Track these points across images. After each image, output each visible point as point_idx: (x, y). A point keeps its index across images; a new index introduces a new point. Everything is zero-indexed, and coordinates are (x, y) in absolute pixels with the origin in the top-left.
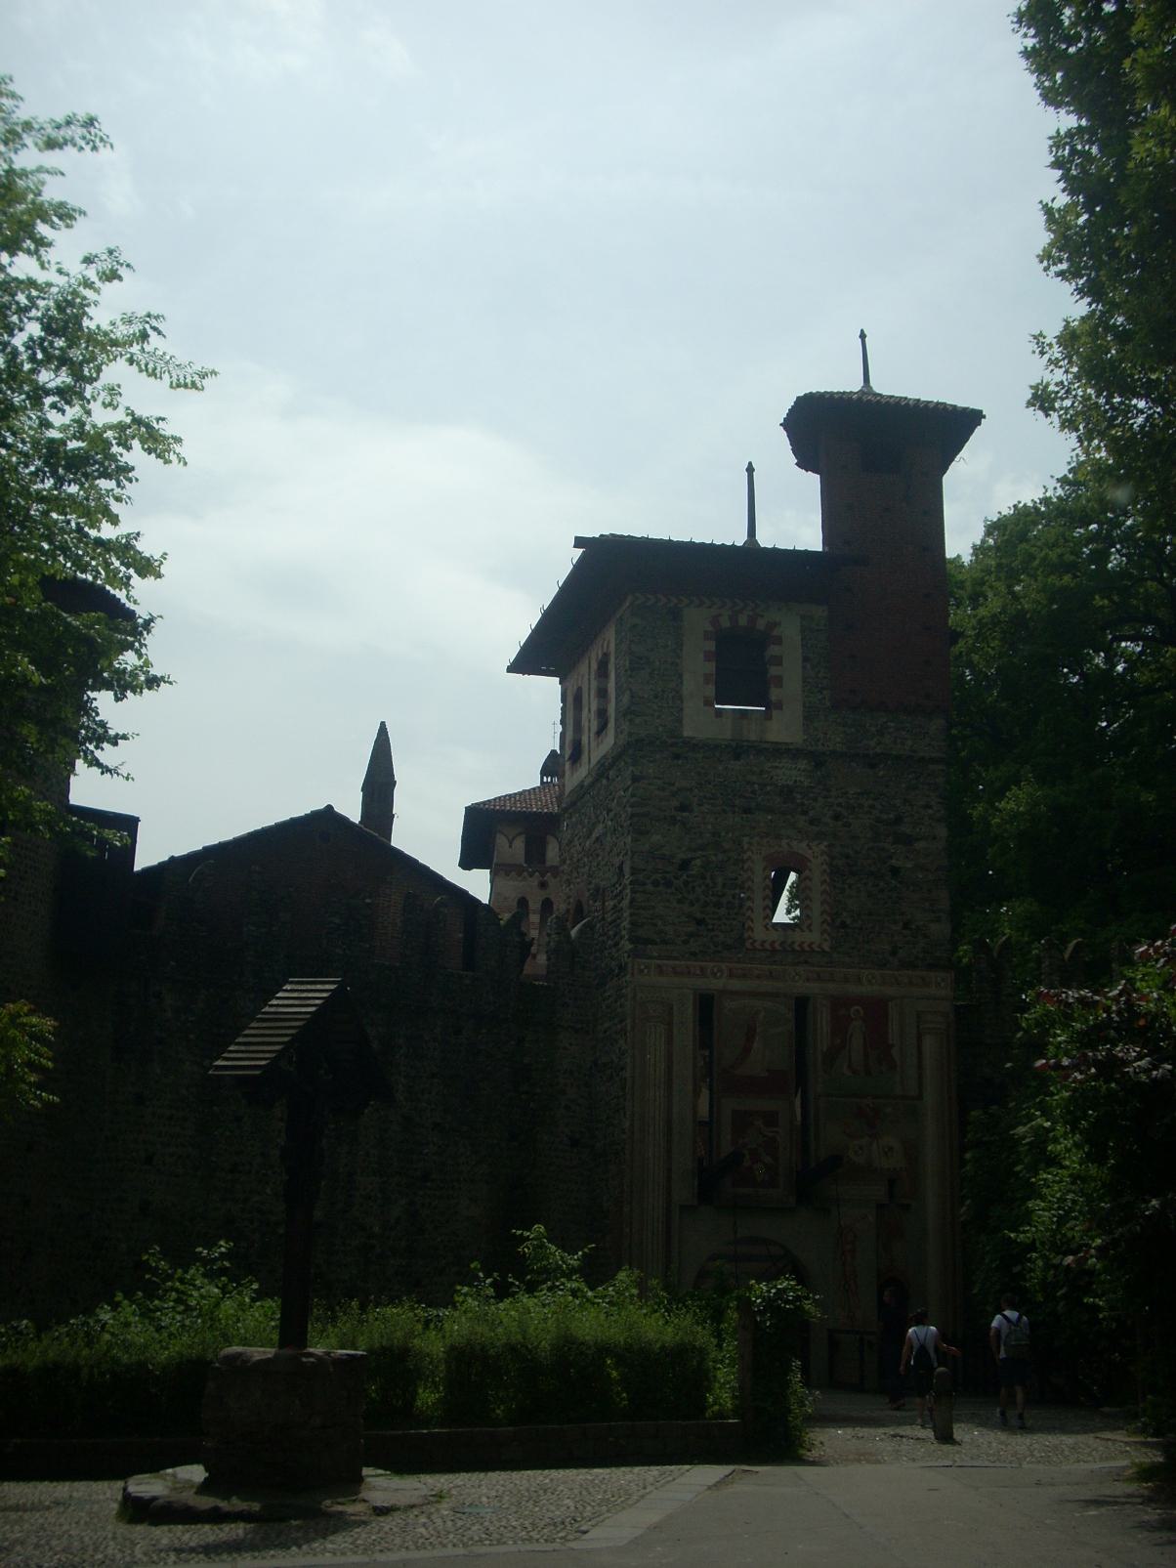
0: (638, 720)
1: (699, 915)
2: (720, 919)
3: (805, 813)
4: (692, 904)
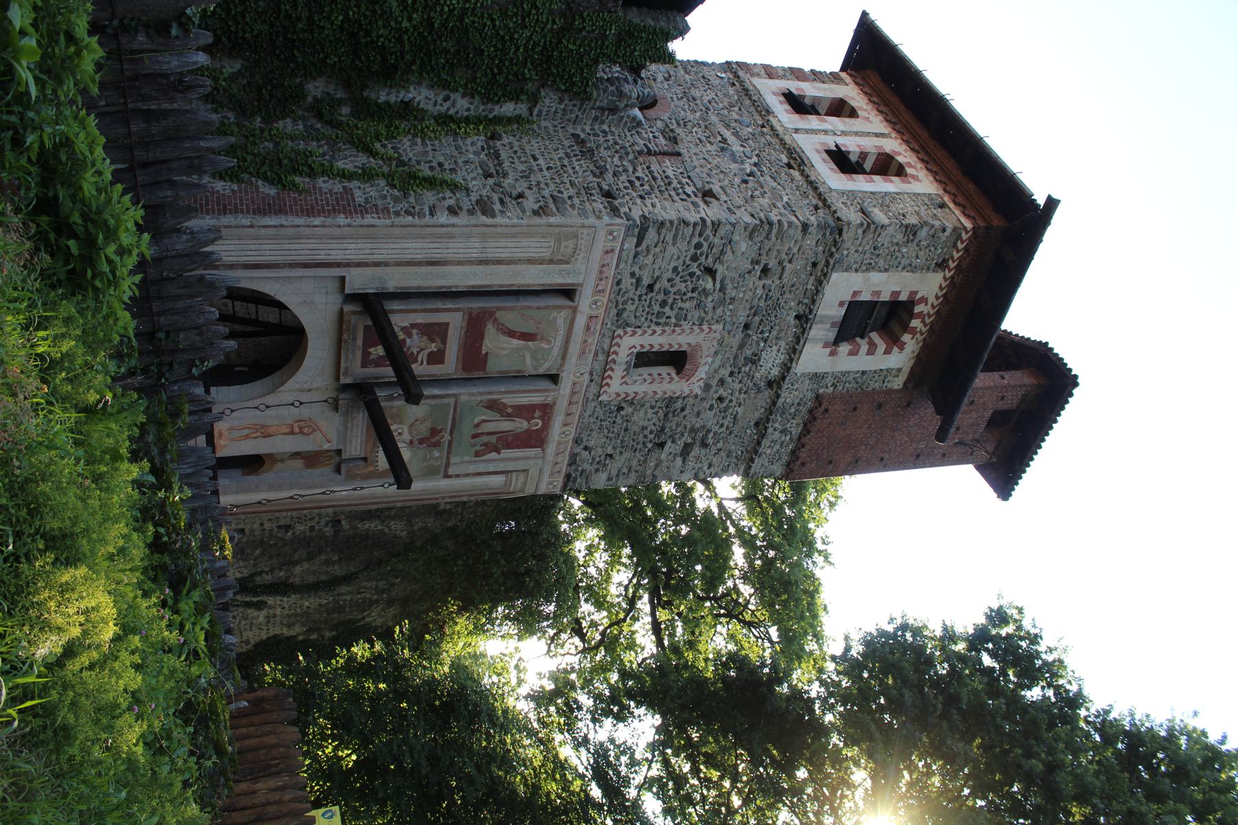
0: (860, 231)
1: (657, 287)
2: (650, 306)
3: (731, 374)
4: (669, 281)
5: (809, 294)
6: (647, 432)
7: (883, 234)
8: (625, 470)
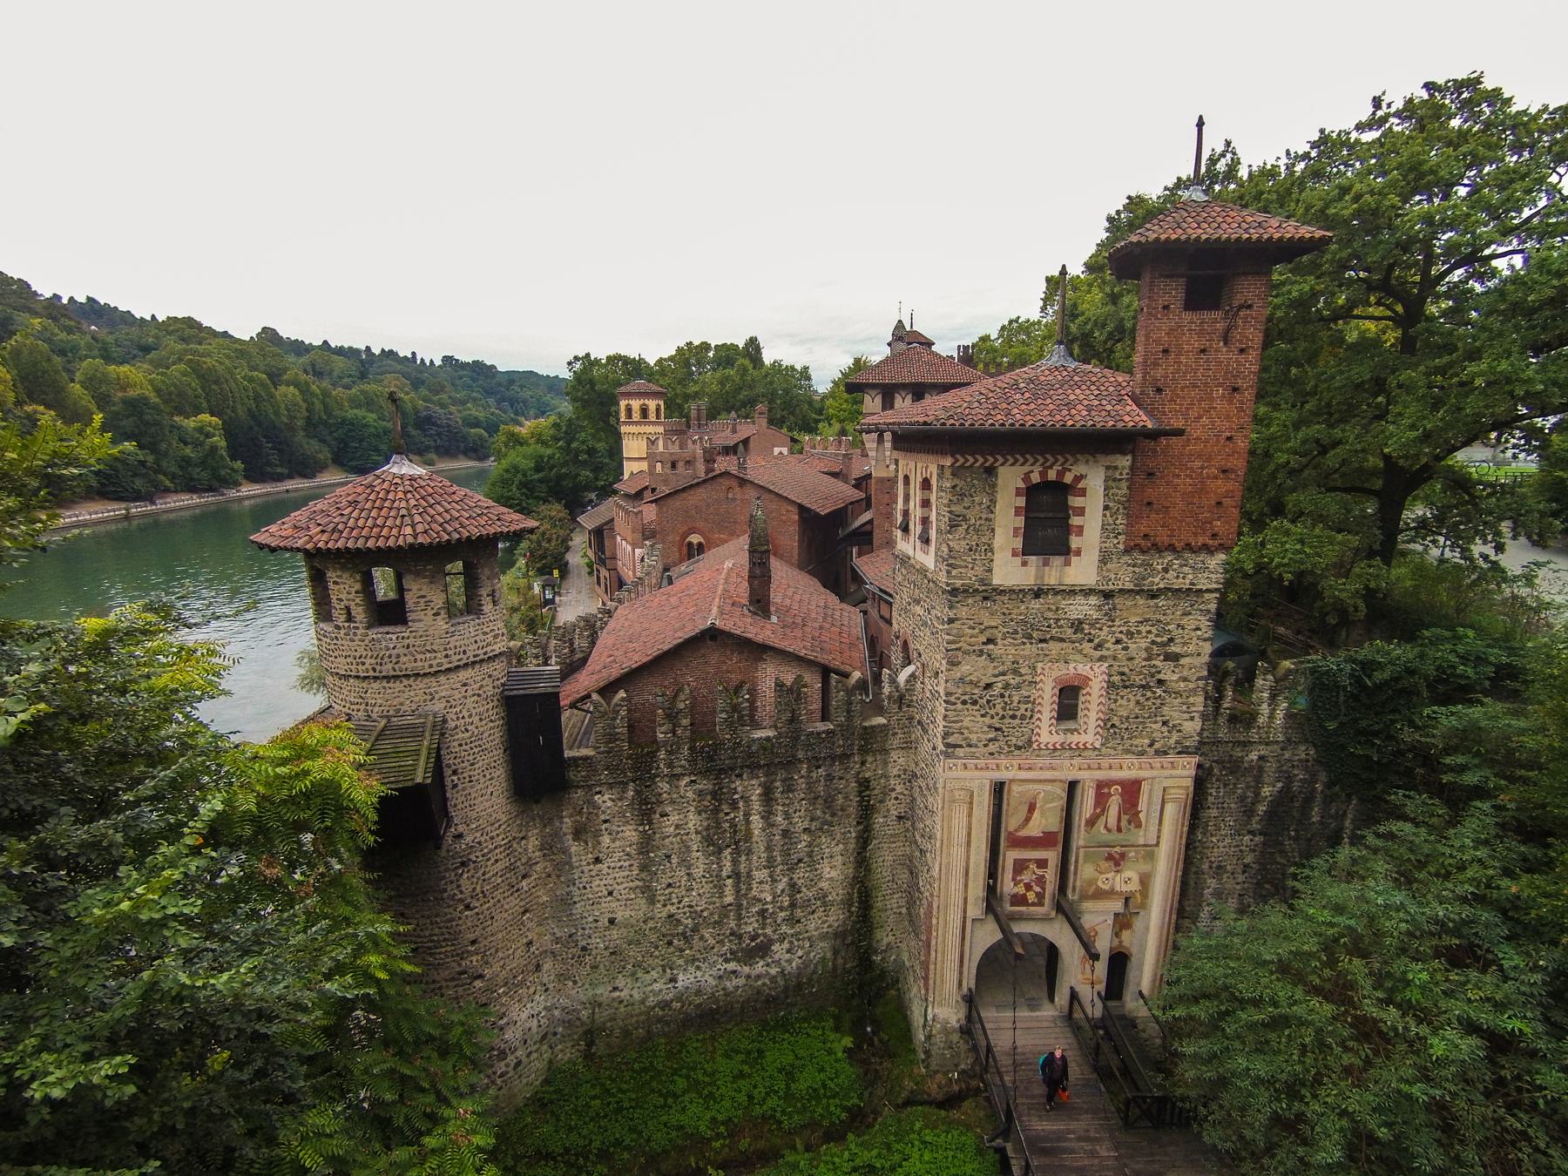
0: (954, 572)
1: (997, 725)
3: (1090, 641)
4: (992, 717)
5: (1014, 596)
6: (1142, 700)
7: (957, 548)
8: (1185, 708)
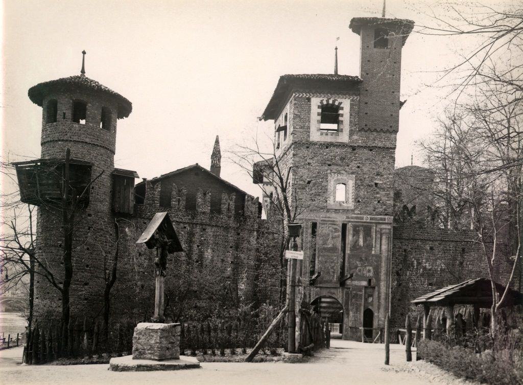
3: (348, 166)
